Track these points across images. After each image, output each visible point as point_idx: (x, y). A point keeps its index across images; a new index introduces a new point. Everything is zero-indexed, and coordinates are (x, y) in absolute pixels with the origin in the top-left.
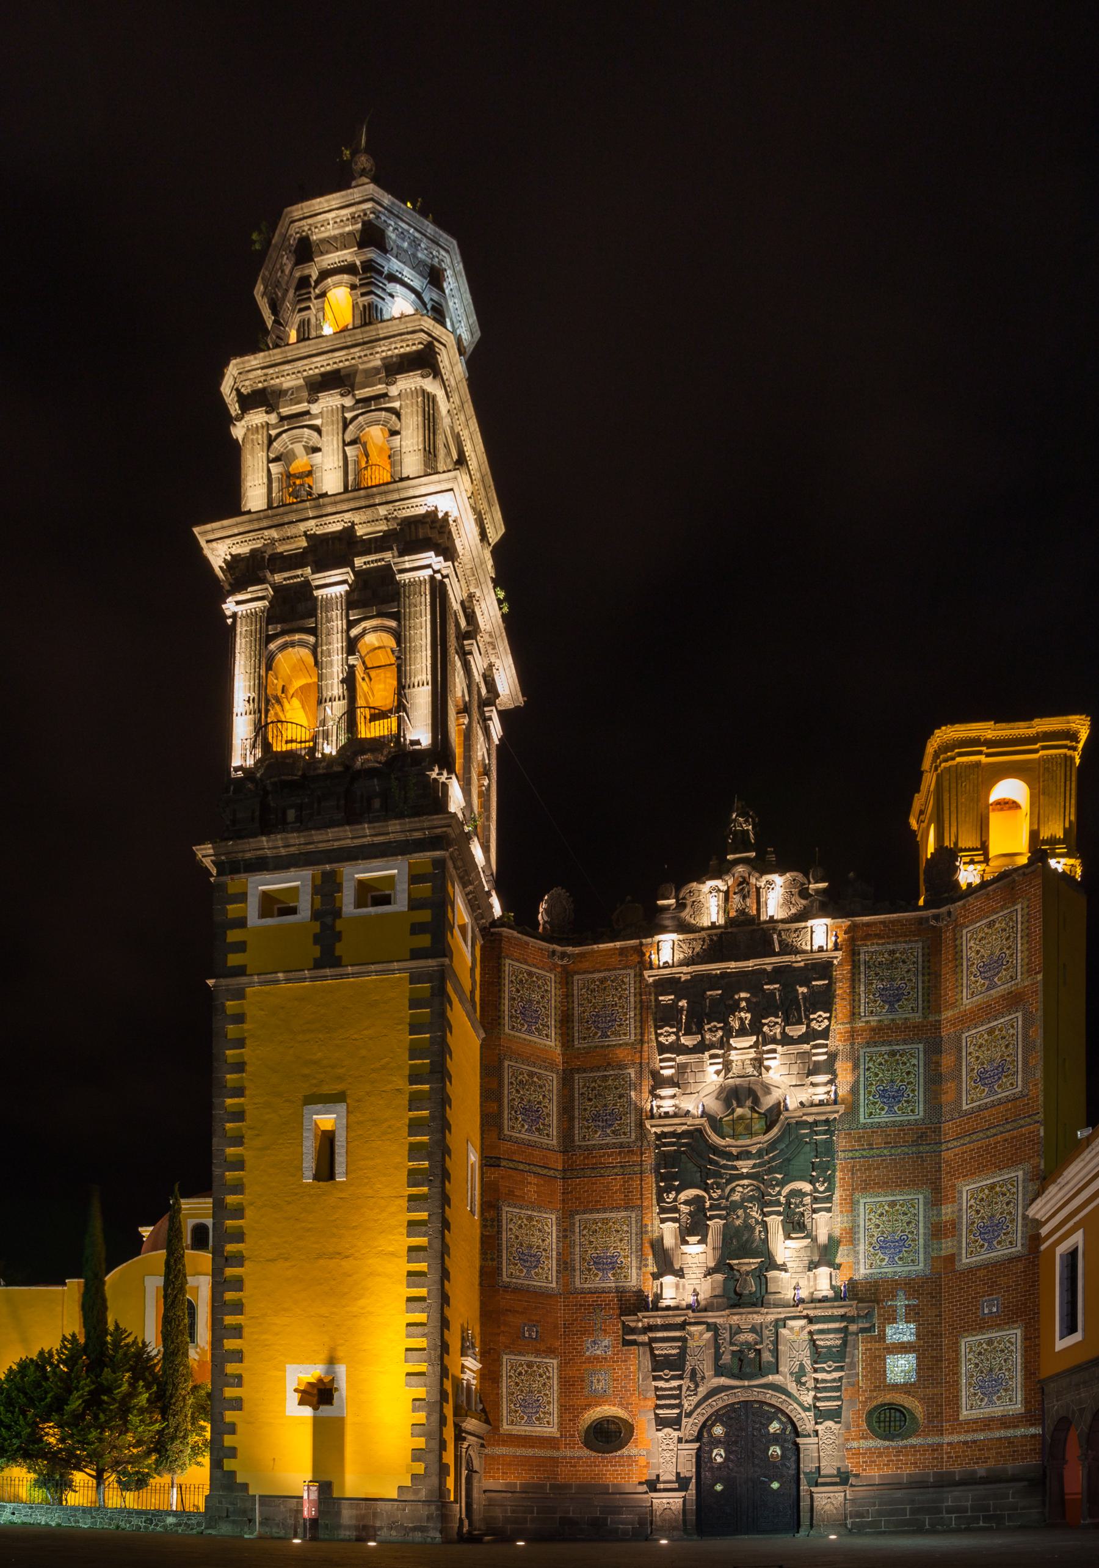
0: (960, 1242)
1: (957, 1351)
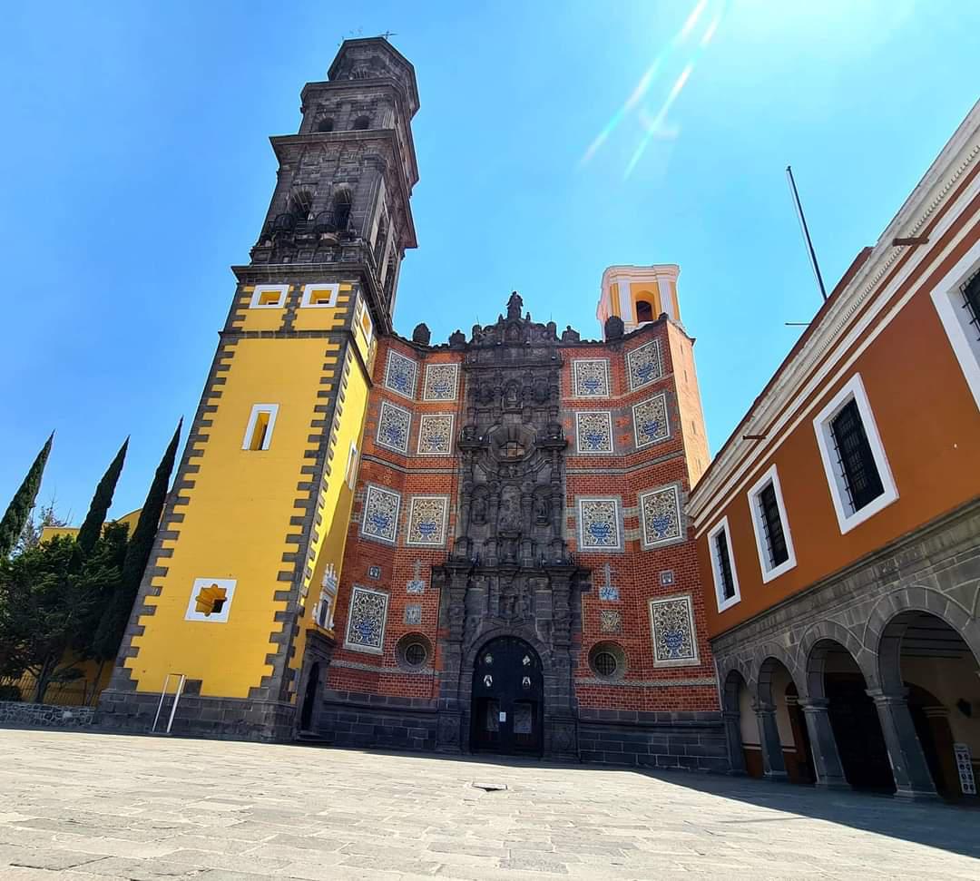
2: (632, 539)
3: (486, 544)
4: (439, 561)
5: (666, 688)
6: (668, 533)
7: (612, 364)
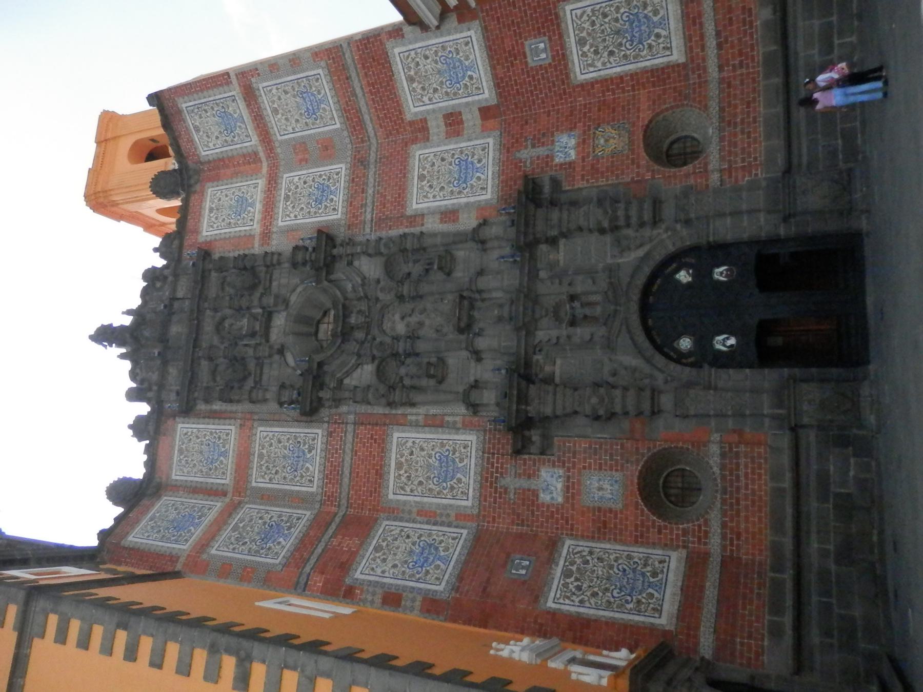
0: (467, 104)
1: (592, 84)
2: (479, 121)
3: (477, 355)
4: (507, 442)
5: (718, 34)
6: (467, 58)
7: (216, 179)
